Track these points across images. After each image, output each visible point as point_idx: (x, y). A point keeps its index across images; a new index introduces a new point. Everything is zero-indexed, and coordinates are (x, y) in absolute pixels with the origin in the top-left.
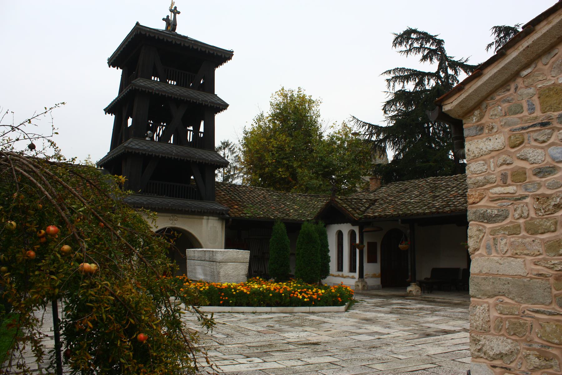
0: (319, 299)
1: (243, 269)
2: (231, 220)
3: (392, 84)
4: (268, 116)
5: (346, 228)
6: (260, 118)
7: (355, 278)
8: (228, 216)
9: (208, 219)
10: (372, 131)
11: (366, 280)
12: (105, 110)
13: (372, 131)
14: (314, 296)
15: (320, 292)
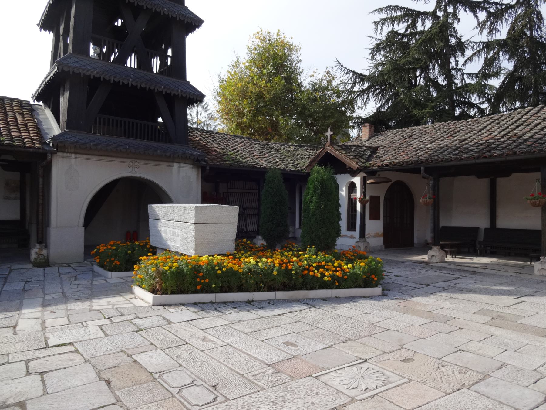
1: (230, 231)
2: (208, 168)
3: (379, 27)
4: (245, 61)
5: (343, 181)
7: (354, 238)
8: (204, 163)
9: (179, 167)
10: (355, 79)
11: (368, 240)
12: (38, 25)
13: (355, 79)
14: (337, 274)
15: (345, 267)
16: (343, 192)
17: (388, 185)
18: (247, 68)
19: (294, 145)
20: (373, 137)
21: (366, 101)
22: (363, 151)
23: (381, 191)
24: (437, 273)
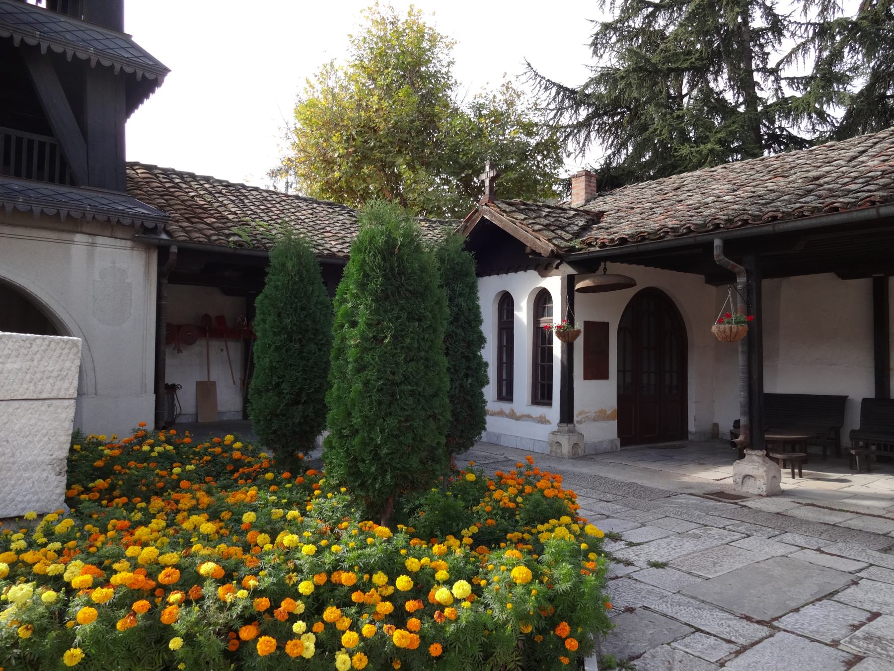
0: (435, 650)
2: (174, 249)
5: (523, 287)
6: (329, 70)
8: (164, 236)
9: (93, 245)
10: (562, 101)
11: (579, 428)
13: (562, 101)
16: (523, 314)
17: (628, 294)
18: (350, 78)
19: (430, 221)
20: (595, 199)
21: (584, 145)
22: (568, 218)
23: (609, 310)
24: (777, 549)
